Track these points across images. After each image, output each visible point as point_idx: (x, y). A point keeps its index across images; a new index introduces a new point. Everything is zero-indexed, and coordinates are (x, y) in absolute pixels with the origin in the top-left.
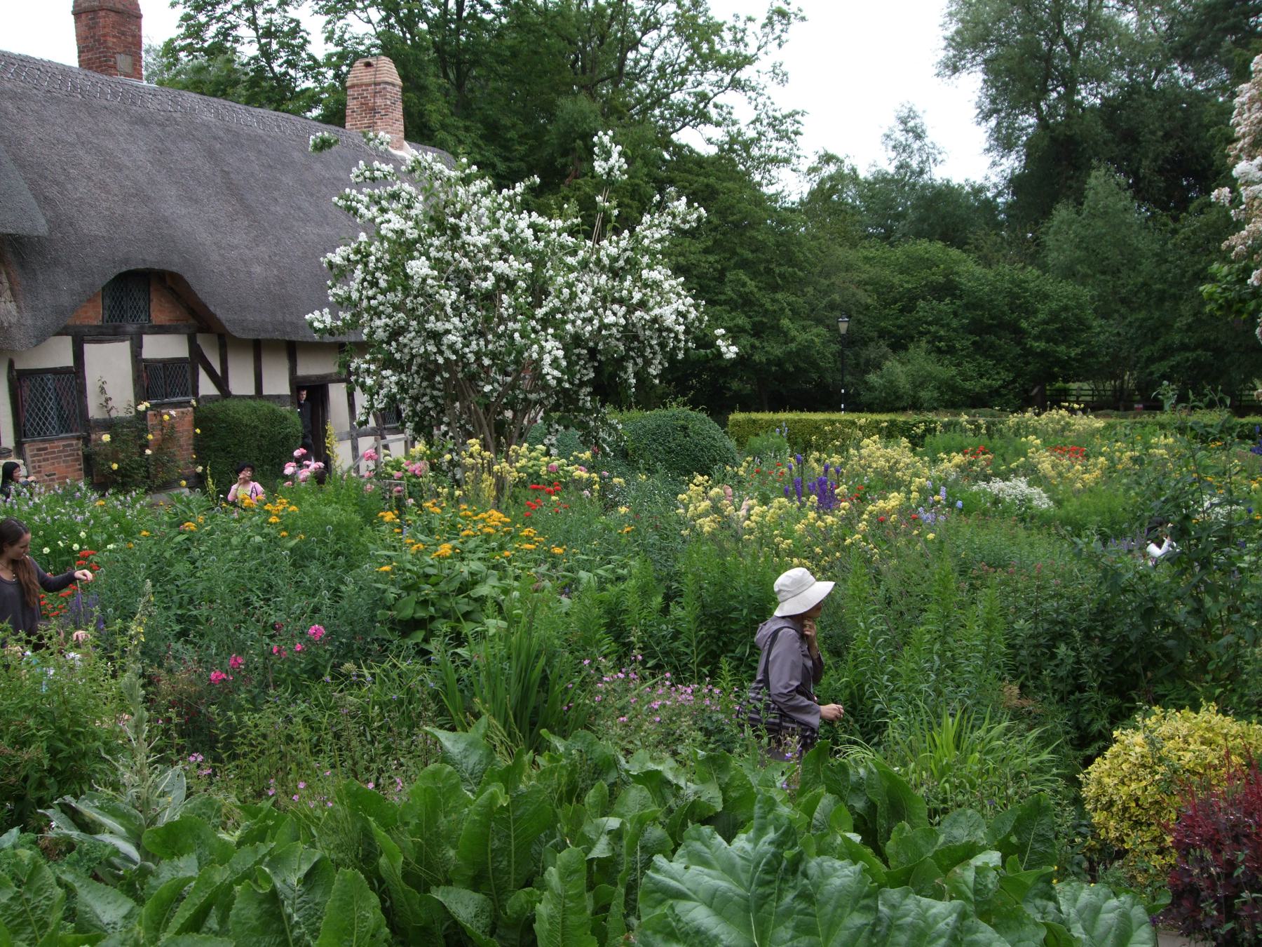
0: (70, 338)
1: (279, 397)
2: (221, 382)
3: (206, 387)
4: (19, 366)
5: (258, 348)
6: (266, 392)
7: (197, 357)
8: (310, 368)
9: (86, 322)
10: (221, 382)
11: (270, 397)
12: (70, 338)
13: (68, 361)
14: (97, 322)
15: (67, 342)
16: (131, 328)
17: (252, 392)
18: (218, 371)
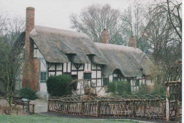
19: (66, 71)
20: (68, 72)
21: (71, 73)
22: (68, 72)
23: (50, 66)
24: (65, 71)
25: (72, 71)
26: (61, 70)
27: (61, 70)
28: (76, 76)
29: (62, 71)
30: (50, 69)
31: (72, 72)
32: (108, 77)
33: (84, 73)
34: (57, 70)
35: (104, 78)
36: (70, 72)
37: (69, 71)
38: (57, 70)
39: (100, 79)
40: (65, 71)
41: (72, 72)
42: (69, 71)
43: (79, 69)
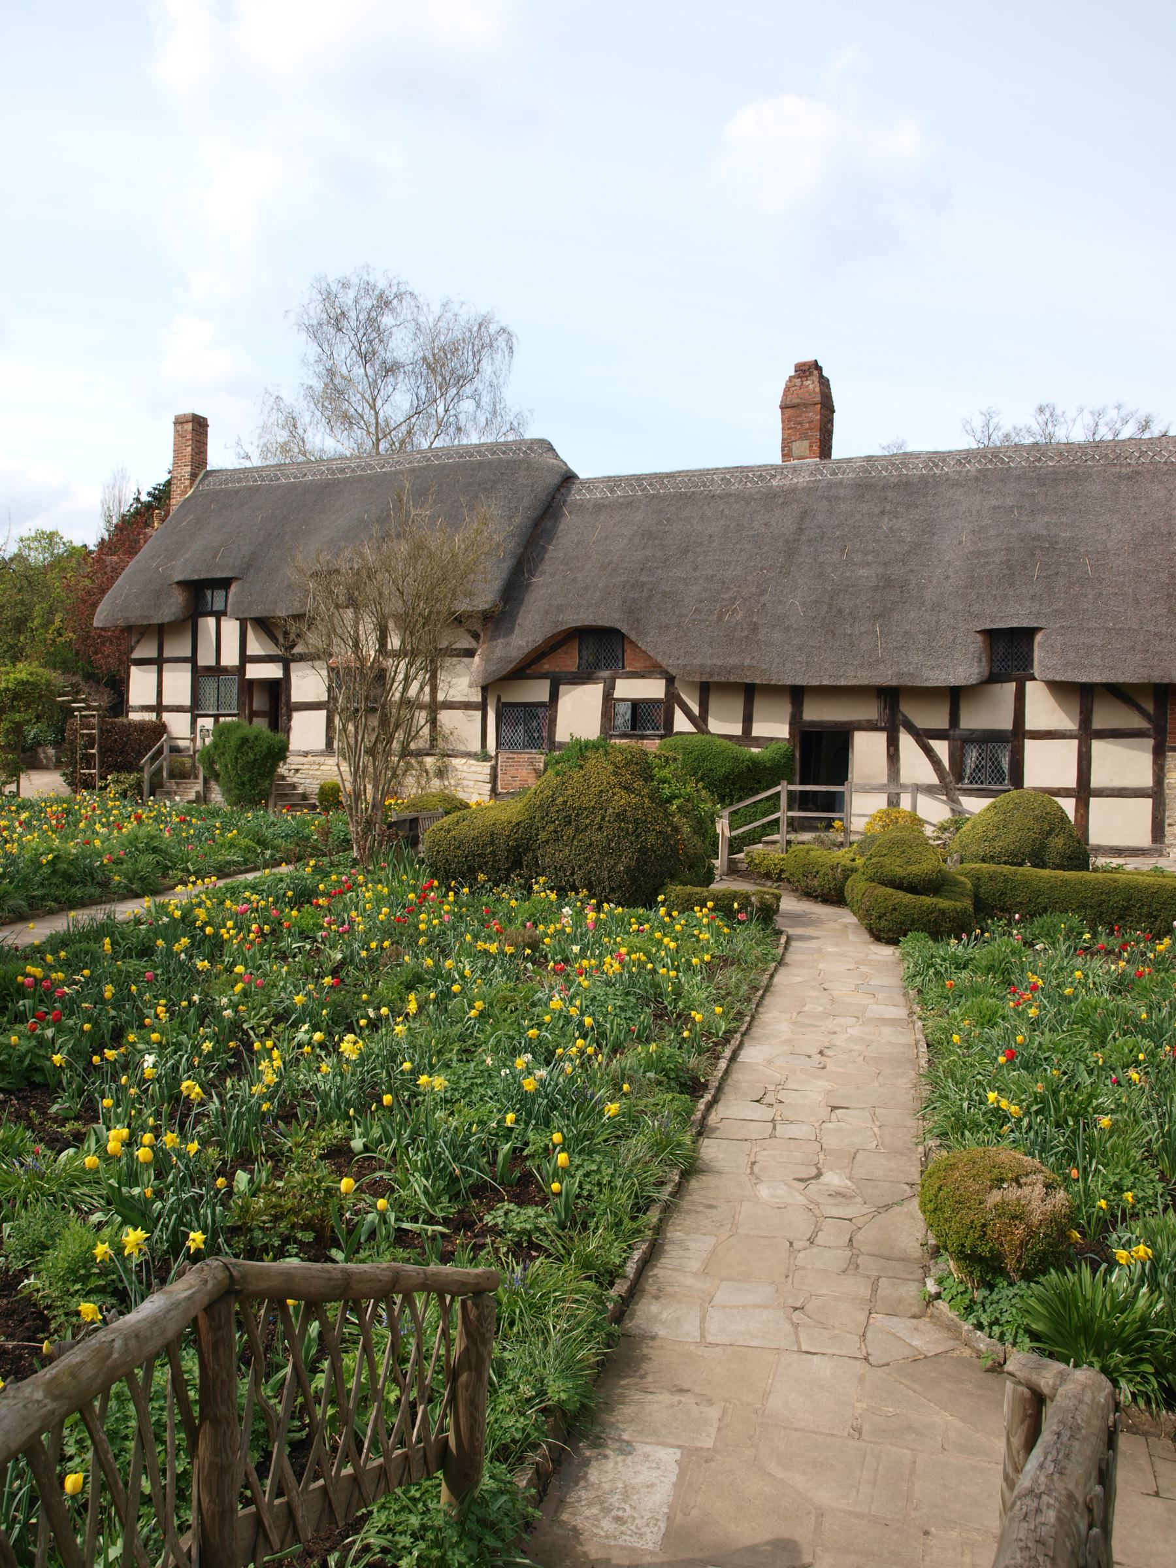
0: (548, 681)
1: (772, 739)
2: (700, 722)
3: (681, 723)
4: (503, 700)
5: (750, 694)
6: (755, 733)
7: (672, 698)
8: (814, 713)
9: (564, 669)
10: (700, 722)
11: (758, 741)
12: (548, 681)
13: (545, 698)
14: (574, 669)
15: (546, 684)
16: (606, 674)
17: (740, 733)
18: (696, 709)
19: (213, 663)
20: (223, 663)
21: (241, 669)
22: (223, 663)
23: (138, 642)
24: (206, 659)
25: (245, 659)
26: (189, 654)
27: (189, 654)
28: (277, 690)
29: (193, 660)
30: (135, 655)
31: (249, 666)
32: (554, 696)
33: (331, 669)
34: (166, 655)
35: (506, 705)
36: (237, 663)
37: (230, 658)
38: (166, 655)
39: (467, 706)
40: (206, 659)
41: (249, 666)
42: (230, 658)
43: (297, 650)
